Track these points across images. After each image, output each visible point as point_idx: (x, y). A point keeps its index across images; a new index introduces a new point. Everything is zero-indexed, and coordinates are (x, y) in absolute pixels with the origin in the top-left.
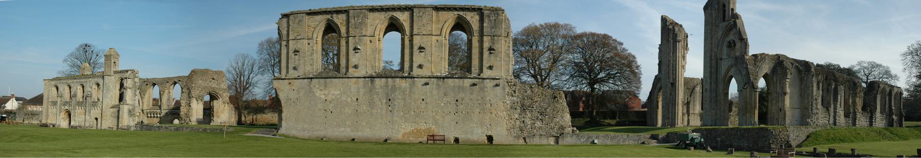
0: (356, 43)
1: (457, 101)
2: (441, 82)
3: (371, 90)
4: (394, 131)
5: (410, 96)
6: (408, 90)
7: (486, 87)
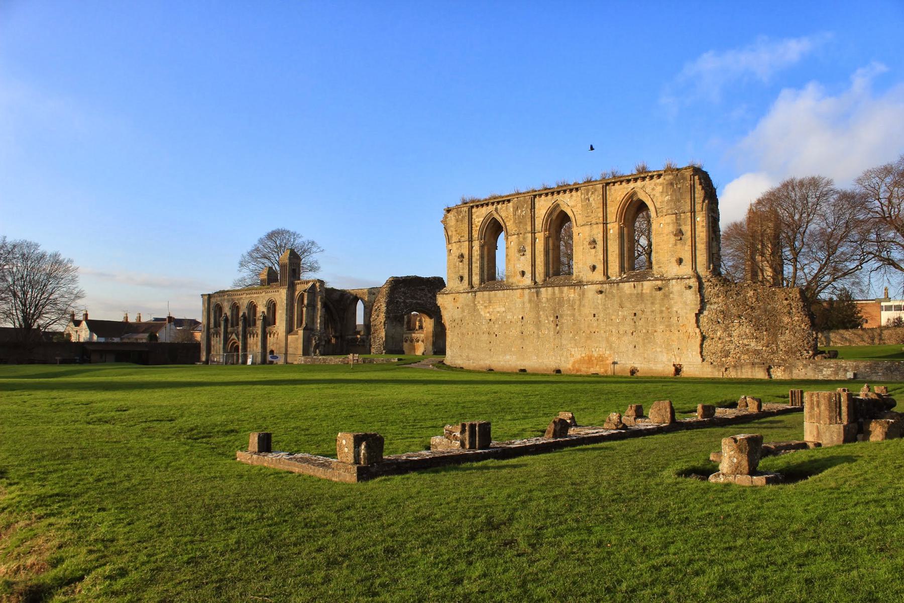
1: (635, 314)
3: (537, 305)
4: (563, 359)
5: (579, 310)
6: (578, 303)
7: (672, 293)
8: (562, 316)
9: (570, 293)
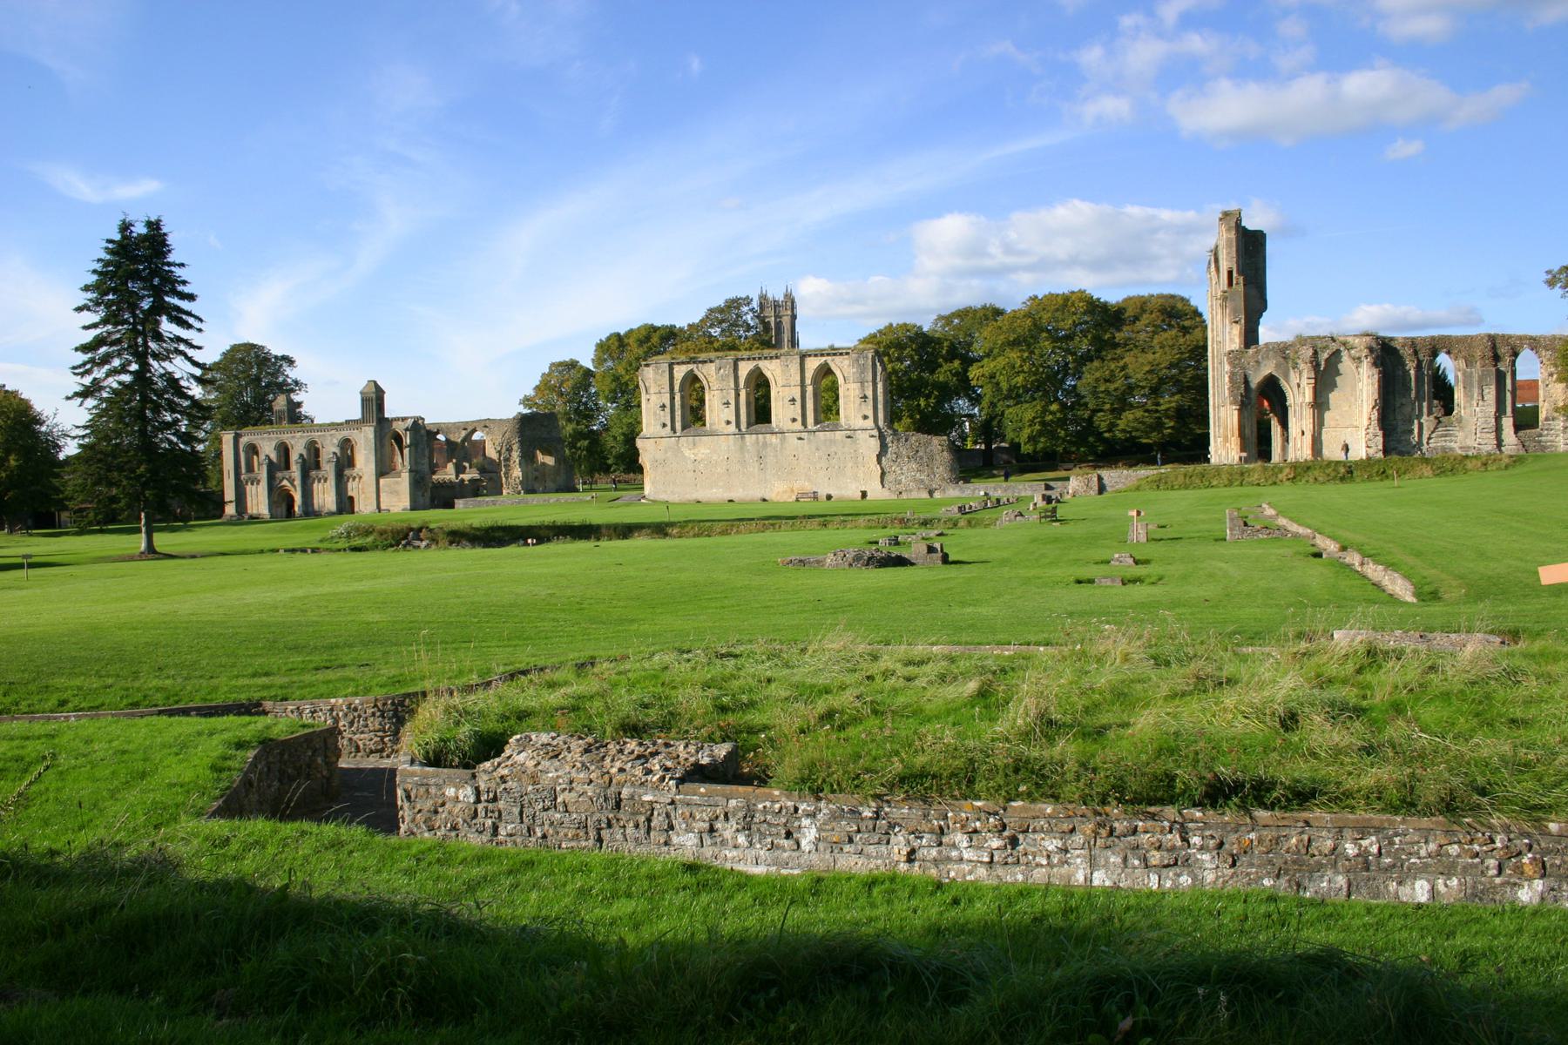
3: (742, 448)
9: (774, 439)
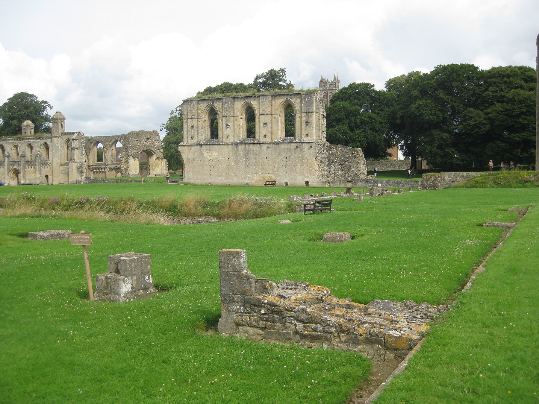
0: (227, 121)
2: (277, 146)
3: (236, 152)
5: (259, 156)
6: (258, 152)
8: (250, 159)
9: (254, 148)
